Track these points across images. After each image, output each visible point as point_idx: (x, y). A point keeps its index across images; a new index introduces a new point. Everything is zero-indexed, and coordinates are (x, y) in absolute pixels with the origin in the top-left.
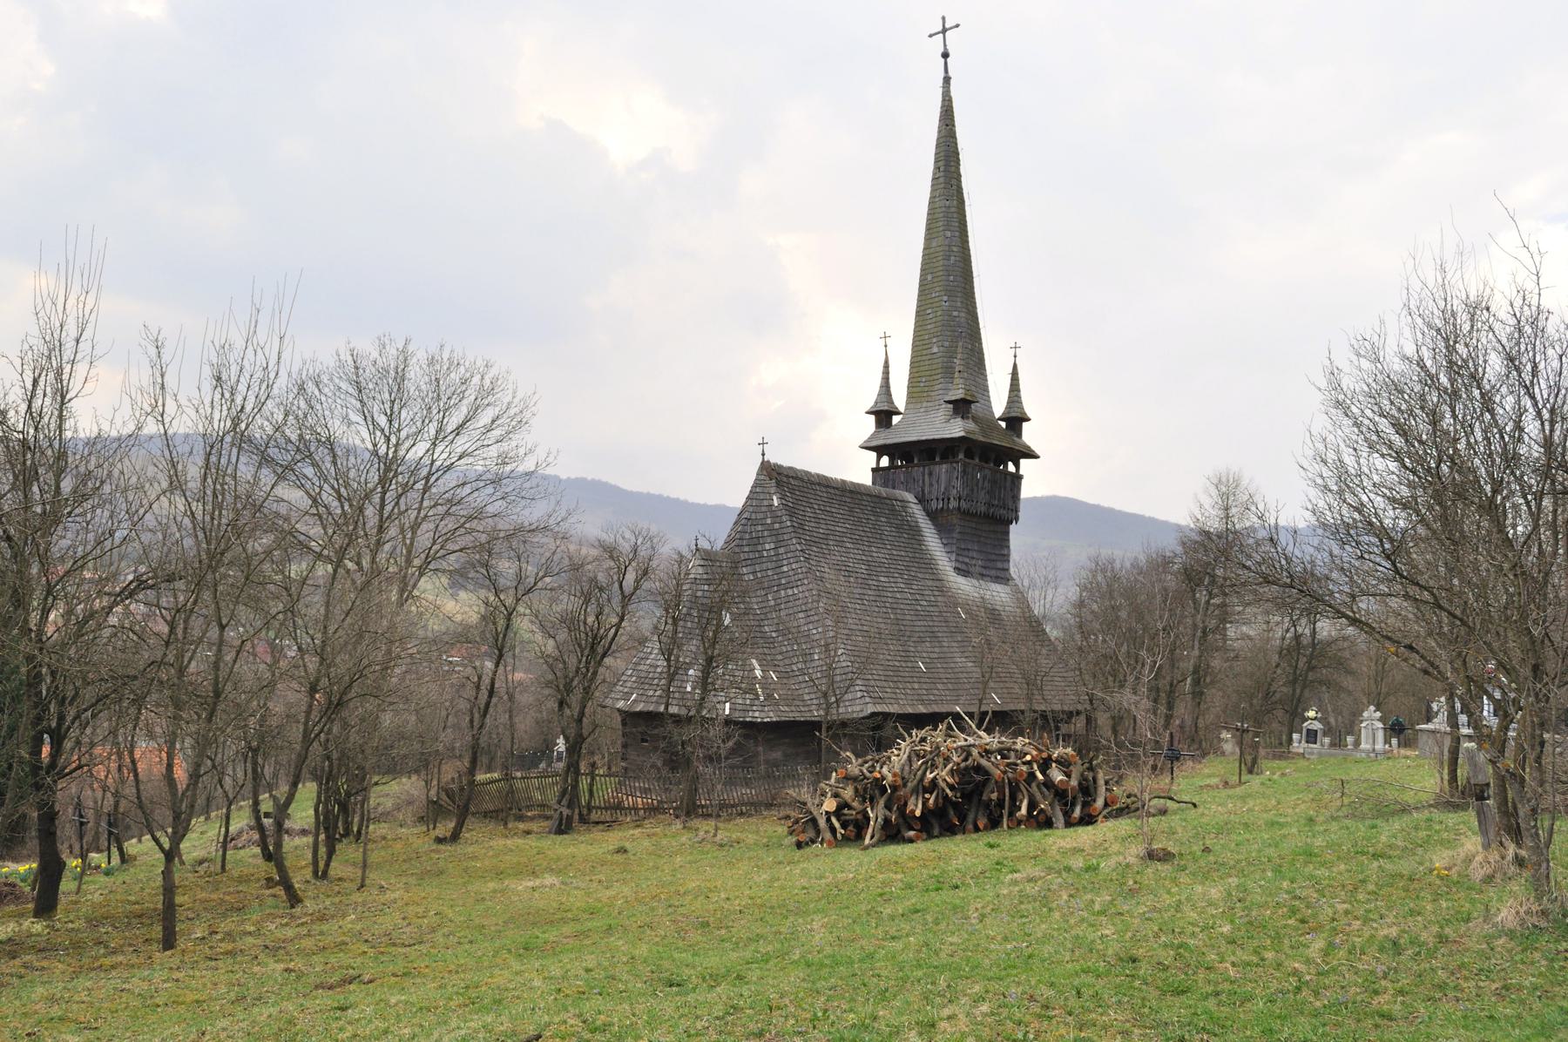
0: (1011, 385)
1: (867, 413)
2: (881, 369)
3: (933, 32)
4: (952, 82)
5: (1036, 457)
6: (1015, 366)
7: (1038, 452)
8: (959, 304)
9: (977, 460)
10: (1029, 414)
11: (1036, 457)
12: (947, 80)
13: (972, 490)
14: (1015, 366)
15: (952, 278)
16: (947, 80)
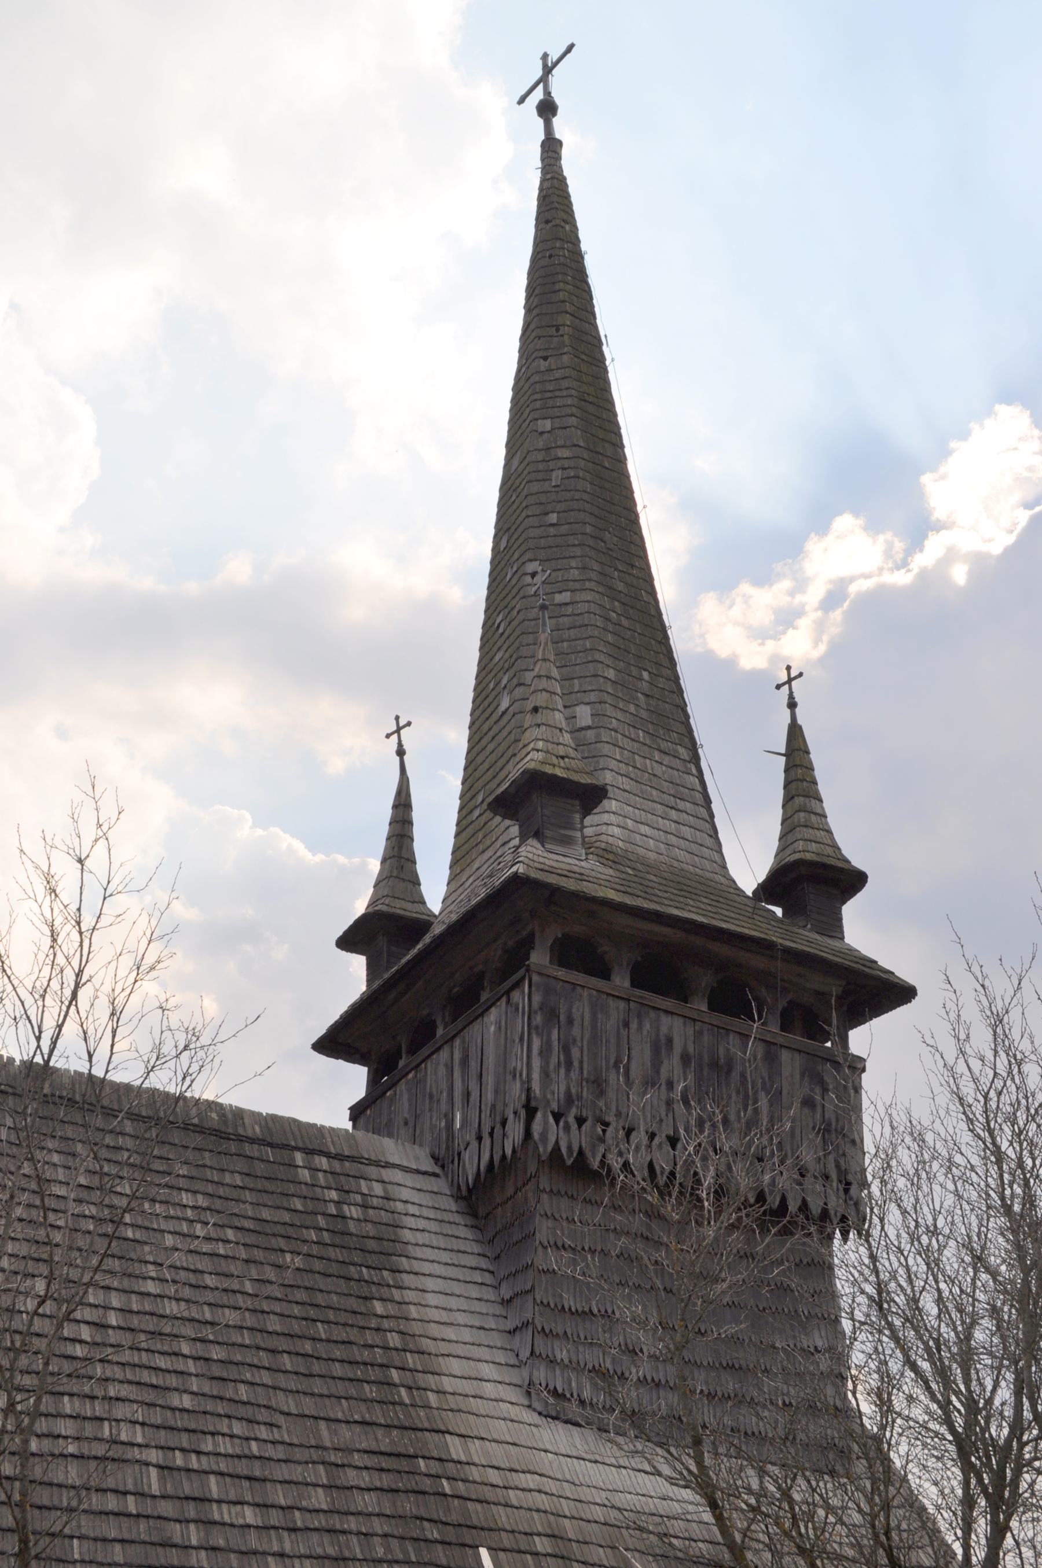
0: (788, 800)
1: (348, 942)
2: (386, 813)
3: (523, 92)
4: (565, 152)
5: (903, 993)
6: (795, 732)
7: (904, 971)
8: (575, 574)
9: (621, 981)
10: (858, 861)
11: (903, 993)
12: (551, 148)
13: (598, 1085)
14: (795, 732)
15: (553, 518)
16: (551, 148)
